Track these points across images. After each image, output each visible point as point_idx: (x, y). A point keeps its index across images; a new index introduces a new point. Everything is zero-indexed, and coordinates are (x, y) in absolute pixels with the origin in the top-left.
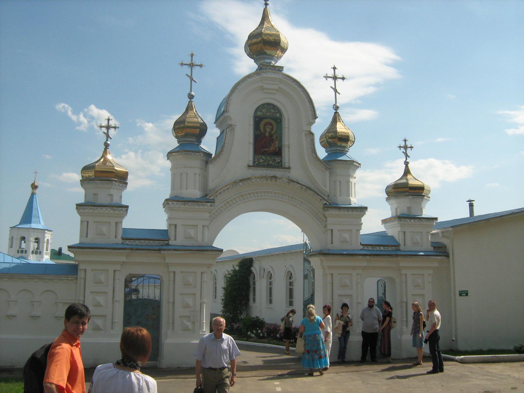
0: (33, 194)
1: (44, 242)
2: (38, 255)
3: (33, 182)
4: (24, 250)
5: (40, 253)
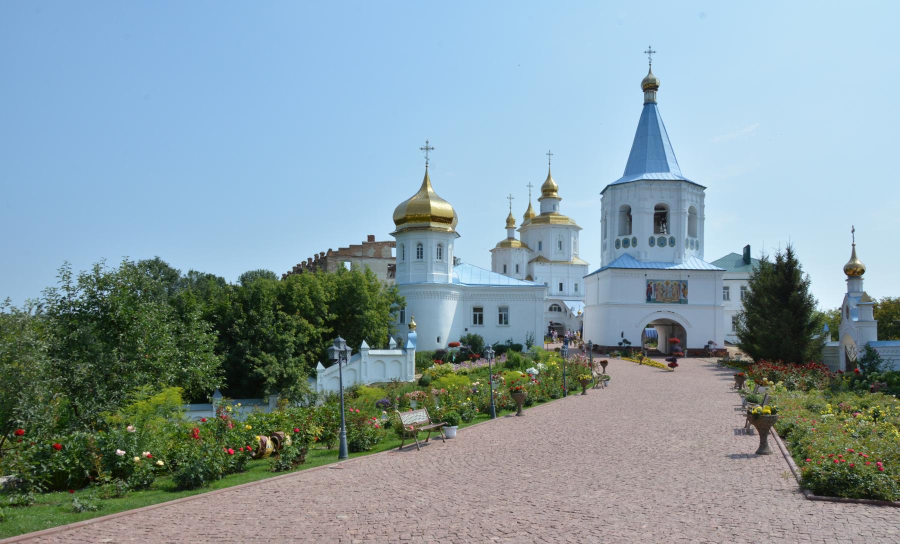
0: (649, 104)
1: (680, 213)
5: (672, 242)
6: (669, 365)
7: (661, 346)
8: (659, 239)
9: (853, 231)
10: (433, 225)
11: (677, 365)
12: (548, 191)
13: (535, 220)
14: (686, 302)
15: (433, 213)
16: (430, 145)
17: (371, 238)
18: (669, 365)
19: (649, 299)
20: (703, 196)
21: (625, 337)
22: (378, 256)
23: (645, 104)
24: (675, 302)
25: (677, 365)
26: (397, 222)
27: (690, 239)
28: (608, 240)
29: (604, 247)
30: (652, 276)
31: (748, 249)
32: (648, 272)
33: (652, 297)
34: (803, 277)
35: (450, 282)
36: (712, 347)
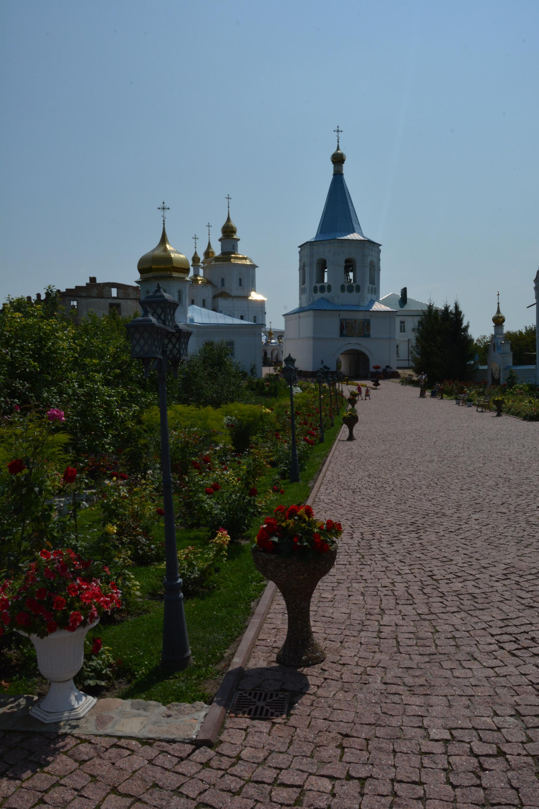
0: (338, 176)
2: (354, 292)
3: (333, 150)
4: (326, 285)
5: (358, 289)
6: (374, 385)
7: (344, 369)
8: (348, 287)
9: (498, 295)
10: (175, 274)
11: (379, 384)
12: (228, 232)
13: (217, 259)
14: (368, 336)
15: (175, 265)
16: (167, 205)
17: (93, 280)
18: (374, 385)
19: (342, 335)
20: (379, 251)
21: (325, 364)
22: (101, 296)
23: (334, 175)
24: (361, 336)
25: (379, 384)
26: (141, 271)
27: (370, 286)
28: (307, 284)
29: (302, 291)
30: (345, 315)
31: (404, 291)
32: (341, 313)
33: (344, 332)
34: (465, 324)
35: (188, 322)
36: (388, 370)
